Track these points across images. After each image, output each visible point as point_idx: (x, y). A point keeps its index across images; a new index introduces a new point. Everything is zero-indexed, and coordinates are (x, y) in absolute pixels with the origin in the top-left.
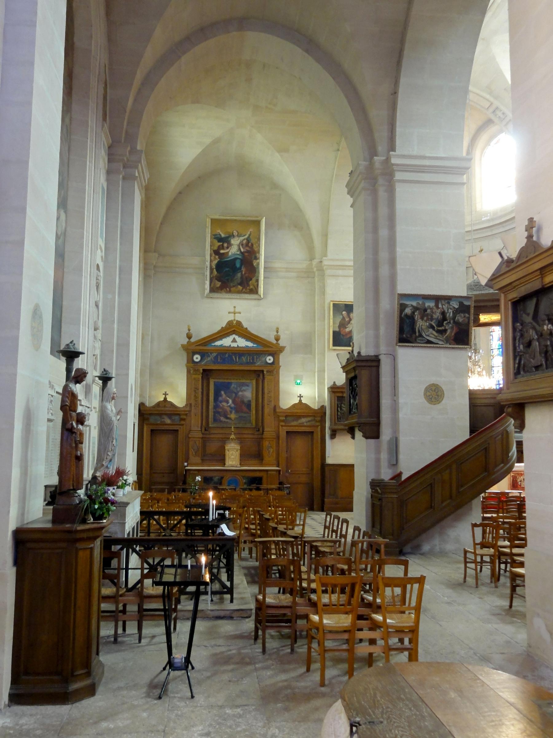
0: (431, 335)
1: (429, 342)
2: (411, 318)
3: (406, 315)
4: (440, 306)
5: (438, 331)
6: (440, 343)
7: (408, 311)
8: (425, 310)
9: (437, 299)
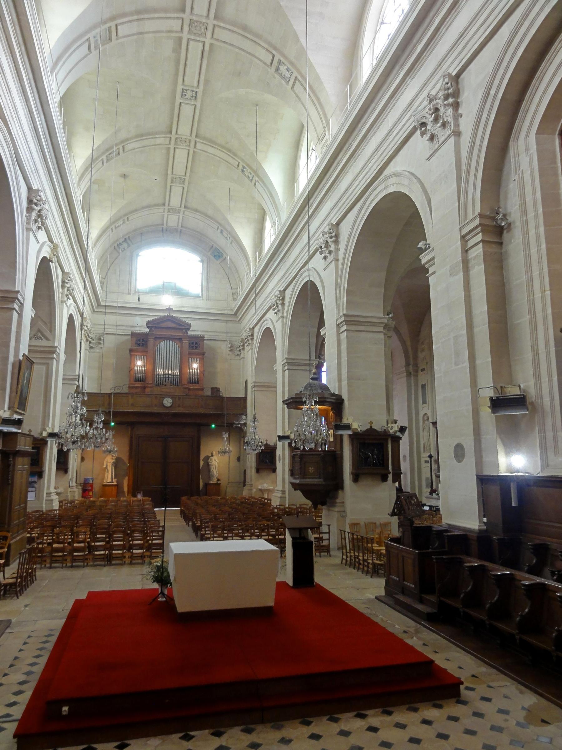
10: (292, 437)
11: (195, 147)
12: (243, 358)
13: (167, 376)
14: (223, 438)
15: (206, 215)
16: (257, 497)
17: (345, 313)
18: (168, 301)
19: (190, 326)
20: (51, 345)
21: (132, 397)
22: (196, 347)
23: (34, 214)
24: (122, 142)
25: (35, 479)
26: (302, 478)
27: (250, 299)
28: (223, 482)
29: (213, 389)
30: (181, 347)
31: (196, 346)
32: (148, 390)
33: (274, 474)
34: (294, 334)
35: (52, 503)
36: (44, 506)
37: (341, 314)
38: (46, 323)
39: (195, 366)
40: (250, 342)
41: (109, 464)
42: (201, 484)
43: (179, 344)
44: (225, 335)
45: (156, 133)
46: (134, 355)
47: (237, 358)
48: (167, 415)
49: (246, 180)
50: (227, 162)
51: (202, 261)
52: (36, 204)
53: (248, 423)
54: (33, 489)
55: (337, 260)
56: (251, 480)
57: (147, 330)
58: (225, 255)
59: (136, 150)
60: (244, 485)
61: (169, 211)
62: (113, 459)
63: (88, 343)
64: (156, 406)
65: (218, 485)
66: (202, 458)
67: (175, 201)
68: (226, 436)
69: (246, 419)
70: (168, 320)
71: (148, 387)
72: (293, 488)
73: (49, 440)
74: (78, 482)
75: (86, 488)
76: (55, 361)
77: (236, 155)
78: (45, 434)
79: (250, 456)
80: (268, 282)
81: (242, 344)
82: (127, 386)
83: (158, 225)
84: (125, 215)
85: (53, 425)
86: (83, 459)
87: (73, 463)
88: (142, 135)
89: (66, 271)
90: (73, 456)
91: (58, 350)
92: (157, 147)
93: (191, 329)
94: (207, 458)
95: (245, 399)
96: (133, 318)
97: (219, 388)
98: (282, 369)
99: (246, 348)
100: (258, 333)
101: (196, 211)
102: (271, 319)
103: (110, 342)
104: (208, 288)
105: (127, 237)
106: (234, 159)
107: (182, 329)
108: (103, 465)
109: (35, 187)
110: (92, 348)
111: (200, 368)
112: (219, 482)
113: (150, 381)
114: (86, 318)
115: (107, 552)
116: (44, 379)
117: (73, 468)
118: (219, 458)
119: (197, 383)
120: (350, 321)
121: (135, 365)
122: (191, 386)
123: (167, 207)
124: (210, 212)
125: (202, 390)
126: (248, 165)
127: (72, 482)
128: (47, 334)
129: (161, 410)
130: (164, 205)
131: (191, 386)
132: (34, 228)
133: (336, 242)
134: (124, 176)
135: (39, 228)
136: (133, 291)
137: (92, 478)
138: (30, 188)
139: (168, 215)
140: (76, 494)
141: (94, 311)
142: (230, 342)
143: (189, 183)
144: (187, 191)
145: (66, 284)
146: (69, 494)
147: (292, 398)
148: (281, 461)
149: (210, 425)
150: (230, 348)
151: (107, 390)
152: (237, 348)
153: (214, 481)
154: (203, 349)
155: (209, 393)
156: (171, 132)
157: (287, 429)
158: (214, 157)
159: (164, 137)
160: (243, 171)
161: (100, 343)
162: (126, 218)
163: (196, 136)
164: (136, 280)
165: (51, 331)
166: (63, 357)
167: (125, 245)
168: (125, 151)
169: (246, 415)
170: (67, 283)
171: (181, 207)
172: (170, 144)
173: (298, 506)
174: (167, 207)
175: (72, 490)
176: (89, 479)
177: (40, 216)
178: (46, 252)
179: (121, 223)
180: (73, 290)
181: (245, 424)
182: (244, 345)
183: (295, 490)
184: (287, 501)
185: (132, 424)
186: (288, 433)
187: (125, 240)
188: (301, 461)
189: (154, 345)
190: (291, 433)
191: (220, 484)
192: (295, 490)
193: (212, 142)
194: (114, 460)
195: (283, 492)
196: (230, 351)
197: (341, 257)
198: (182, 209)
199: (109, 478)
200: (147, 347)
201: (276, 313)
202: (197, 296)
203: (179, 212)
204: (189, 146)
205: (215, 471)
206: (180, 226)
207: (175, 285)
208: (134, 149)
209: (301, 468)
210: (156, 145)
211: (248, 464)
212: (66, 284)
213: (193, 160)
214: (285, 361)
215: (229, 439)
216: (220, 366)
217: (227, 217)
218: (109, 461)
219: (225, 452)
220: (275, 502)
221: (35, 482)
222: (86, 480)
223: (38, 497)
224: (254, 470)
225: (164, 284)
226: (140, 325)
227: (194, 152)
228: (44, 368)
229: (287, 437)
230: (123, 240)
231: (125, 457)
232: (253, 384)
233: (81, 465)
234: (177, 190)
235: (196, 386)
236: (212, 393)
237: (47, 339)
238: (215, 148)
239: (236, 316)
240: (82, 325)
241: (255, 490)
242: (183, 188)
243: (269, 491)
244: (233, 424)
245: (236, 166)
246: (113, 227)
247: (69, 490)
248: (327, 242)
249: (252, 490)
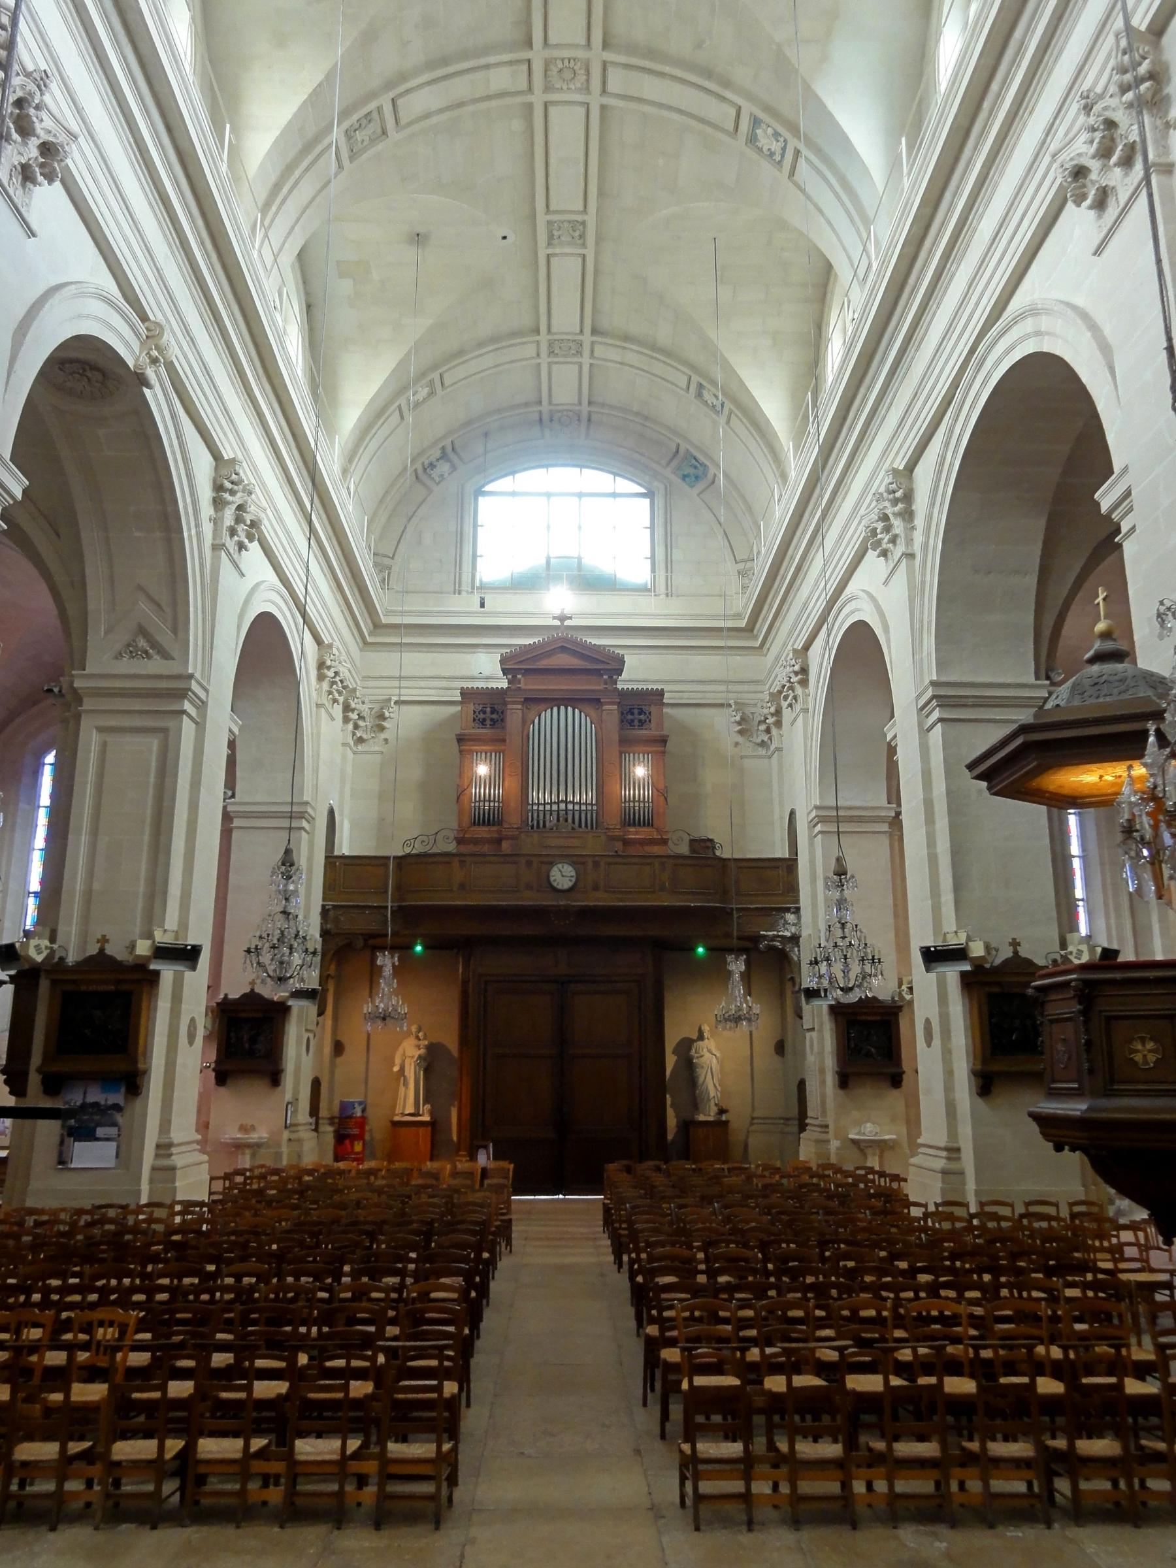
10: (977, 950)
11: (604, 91)
12: (778, 749)
13: (563, 806)
14: (730, 974)
15: (654, 348)
16: (849, 1167)
18: (559, 603)
19: (621, 661)
20: (175, 672)
21: (462, 862)
22: (642, 723)
24: (389, 85)
25: (118, 1098)
26: (1094, 1094)
27: (792, 558)
28: (737, 1119)
29: (693, 842)
30: (599, 723)
31: (638, 718)
32: (505, 845)
33: (895, 1093)
34: (958, 604)
35: (173, 1181)
36: (145, 1187)
38: (159, 605)
39: (640, 771)
40: (799, 690)
41: (407, 1062)
42: (672, 1121)
43: (592, 713)
44: (723, 688)
45: (487, 50)
46: (471, 752)
47: (762, 751)
48: (563, 912)
49: (766, 167)
50: (702, 121)
51: (650, 495)
53: (804, 934)
54: (112, 1131)
56: (824, 1112)
57: (504, 684)
58: (712, 470)
59: (434, 120)
60: (802, 1127)
61: (551, 353)
62: (418, 1047)
63: (350, 726)
64: (529, 887)
65: (720, 1126)
66: (669, 1047)
67: (566, 318)
68: (737, 966)
69: (797, 924)
70: (563, 649)
71: (507, 838)
72: (1046, 1136)
73: (167, 972)
74: (323, 1112)
75: (347, 1129)
76: (188, 728)
77: (727, 84)
78: (143, 948)
79: (814, 1034)
80: (848, 479)
81: (773, 710)
82: (452, 835)
83: (527, 404)
84: (435, 367)
85: (184, 924)
86: (338, 1048)
87: (298, 1057)
88: (445, 61)
90: (299, 1037)
91: (194, 686)
92: (494, 103)
93: (624, 675)
94: (686, 1046)
95: (789, 865)
96: (469, 656)
97: (711, 841)
98: (920, 724)
99: (787, 714)
100: (821, 660)
101: (627, 338)
102: (863, 591)
103: (407, 722)
104: (669, 563)
105: (447, 443)
106: (723, 99)
107: (598, 673)
108: (393, 1065)
110: (361, 740)
111: (654, 776)
112: (724, 1118)
113: (514, 820)
114: (330, 646)
115: (174, 1446)
116: (152, 779)
117: (298, 1069)
118: (720, 1043)
119: (649, 823)
121: (473, 779)
122: (633, 833)
123: (543, 337)
124: (664, 335)
125: (664, 842)
126: (768, 109)
127: (295, 1112)
128: (165, 638)
129: (548, 901)
130: (537, 331)
131: (633, 833)
134: (418, 239)
136: (466, 586)
137: (360, 1103)
139: (550, 364)
140: (312, 1150)
141: (365, 643)
142: (740, 706)
143: (599, 239)
144: (596, 272)
145: (227, 496)
146: (285, 1150)
147: (1023, 729)
148: (937, 1041)
149: (693, 949)
150: (739, 723)
151: (396, 850)
152: (760, 722)
153: (708, 1115)
154: (660, 725)
155: (684, 849)
156: (529, 44)
157: (949, 922)
158: (665, 113)
159: (511, 63)
160: (752, 139)
161: (382, 729)
162: (435, 376)
163: (606, 45)
164: (475, 557)
165: (175, 631)
166: (221, 719)
167: (444, 468)
168: (403, 122)
169: (798, 909)
170: (233, 493)
171: (581, 331)
172: (530, 89)
173: (1020, 1209)
174: (543, 337)
175: (293, 1136)
176: (353, 1103)
179: (424, 392)
180: (254, 524)
181: (795, 939)
182: (778, 713)
183: (1059, 1148)
184: (971, 1186)
185: (464, 946)
186: (956, 939)
187: (444, 456)
188: (1085, 1012)
189: (524, 722)
190: (969, 939)
191: (727, 1122)
192: (1059, 1148)
193: (651, 58)
194: (422, 1051)
195: (953, 1152)
196: (741, 732)
198: (587, 338)
199: (408, 1101)
200: (504, 728)
201: (884, 554)
202: (643, 590)
203: (579, 353)
204: (587, 89)
205: (711, 1083)
206: (585, 402)
207: (580, 559)
208: (427, 116)
209: (1089, 1043)
210: (489, 98)
211: (811, 1059)
212: (227, 496)
213: (603, 151)
214: (929, 693)
215: (746, 977)
216: (711, 778)
217: (712, 334)
218: (410, 1052)
219: (737, 1019)
220: (924, 1190)
221: (117, 1108)
222: (344, 1106)
223: (127, 1158)
224: (830, 1079)
225: (548, 563)
226: (486, 673)
227: (603, 108)
228: (155, 743)
229: (957, 954)
230: (438, 454)
231: (452, 1044)
232: (814, 814)
233: (333, 1065)
234: (566, 269)
235: (642, 833)
236: (692, 849)
237: (166, 656)
238: (662, 75)
239: (751, 632)
240: (321, 665)
241: (835, 1144)
242: (584, 256)
243: (882, 1146)
244: (757, 939)
245: (730, 126)
246: (402, 401)
247: (286, 1135)
248: (1110, 124)
249: (828, 1141)
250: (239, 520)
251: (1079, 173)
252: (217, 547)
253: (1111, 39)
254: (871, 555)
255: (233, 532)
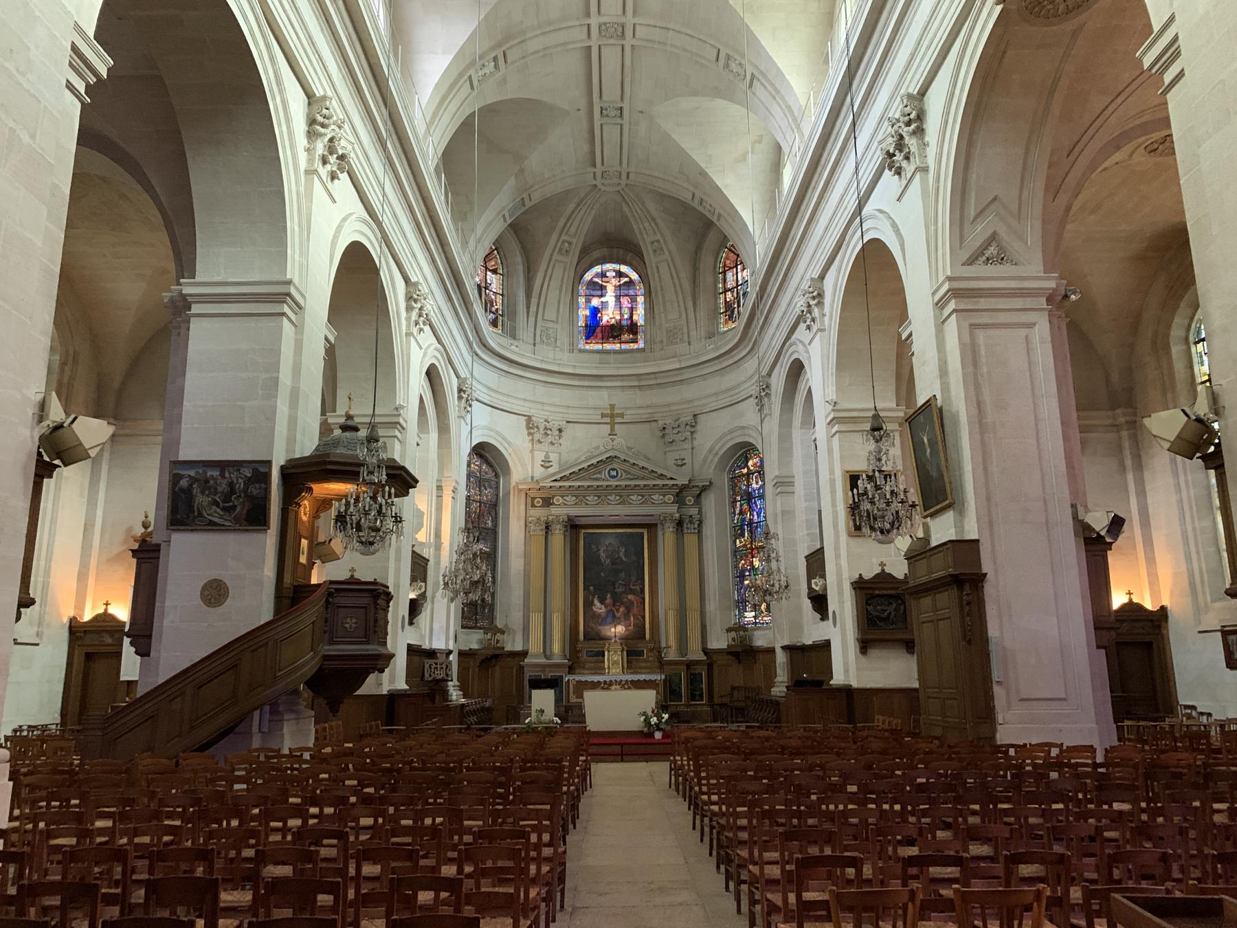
0: (215, 514)
1: (211, 523)
2: (188, 492)
3: (181, 489)
4: (227, 475)
5: (224, 509)
6: (228, 524)
7: (184, 483)
8: (207, 481)
9: (223, 465)
17: (949, 273)
23: (320, 147)
37: (941, 278)
52: (323, 126)
55: (925, 170)
89: (413, 279)
109: (319, 92)
120: (959, 294)
132: (324, 171)
133: (920, 132)
135: (333, 177)
138: (310, 95)
170: (416, 301)
177: (332, 150)
178: (357, 230)
197: (931, 161)
240: (460, 390)
248: (901, 137)
250: (420, 316)
251: (891, 155)
252: (409, 334)
253: (899, 99)
254: (802, 326)
255: (417, 323)
